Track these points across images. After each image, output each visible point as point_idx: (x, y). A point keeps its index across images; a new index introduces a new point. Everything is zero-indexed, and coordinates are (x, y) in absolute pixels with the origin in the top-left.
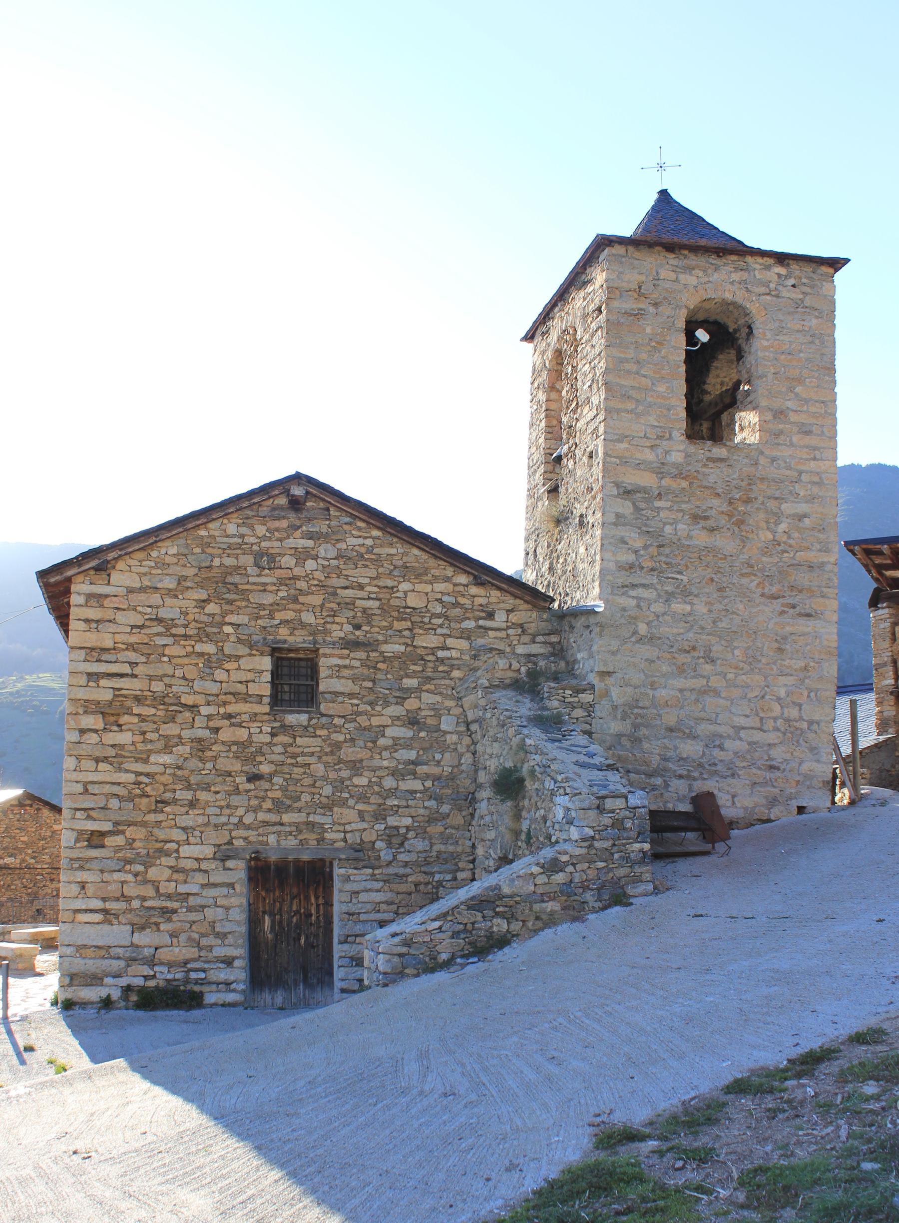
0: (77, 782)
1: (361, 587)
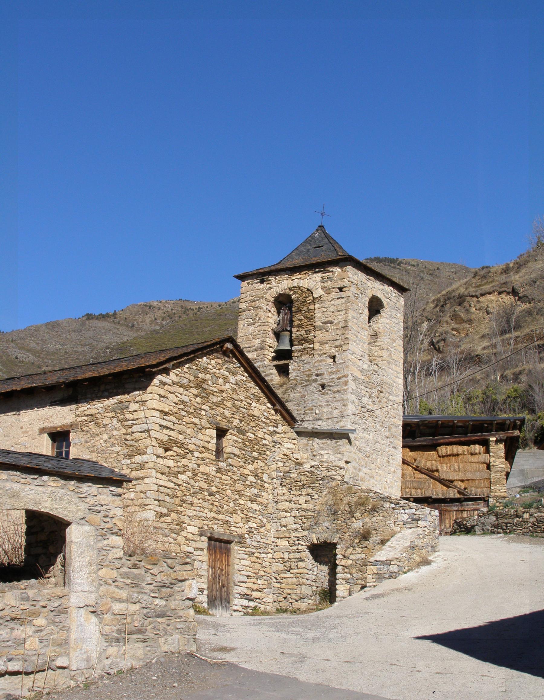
0: (156, 485)
1: (242, 401)
